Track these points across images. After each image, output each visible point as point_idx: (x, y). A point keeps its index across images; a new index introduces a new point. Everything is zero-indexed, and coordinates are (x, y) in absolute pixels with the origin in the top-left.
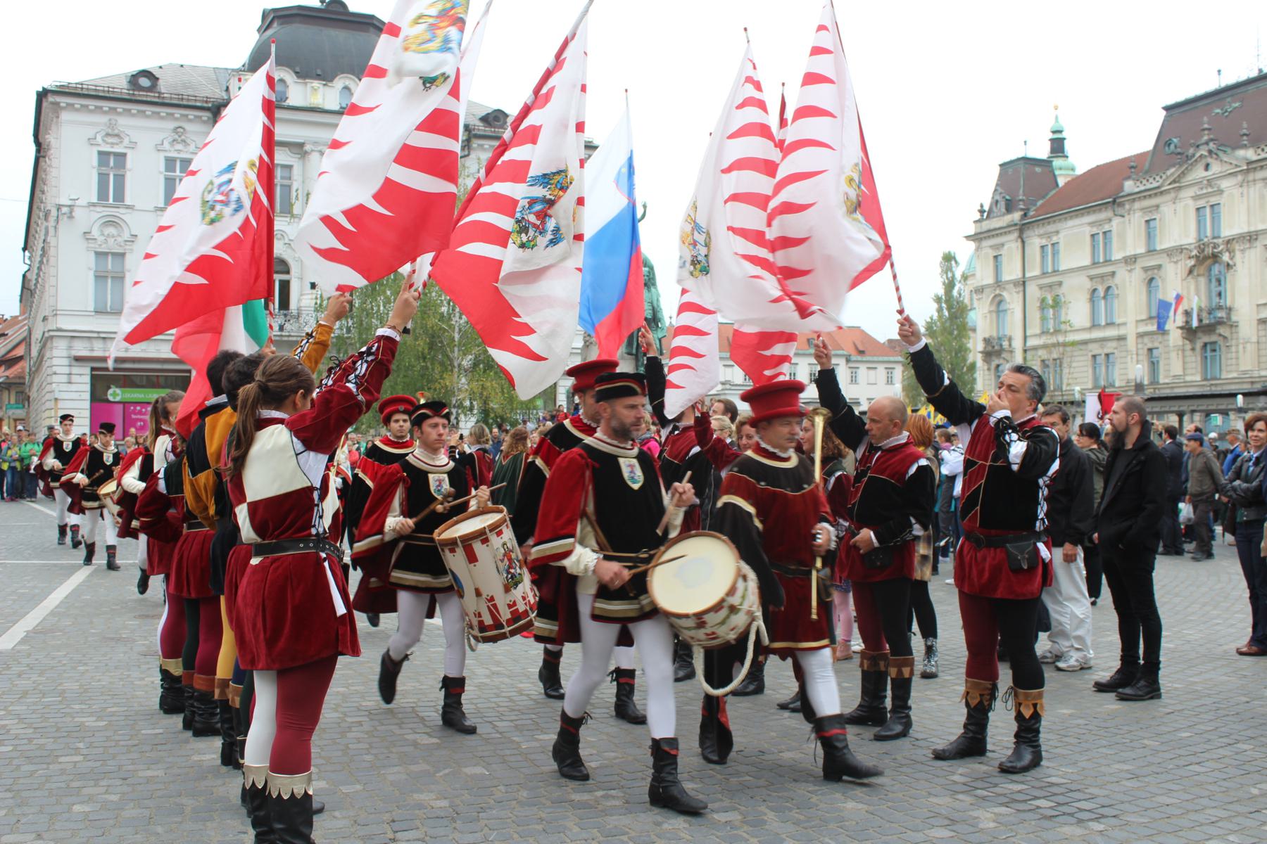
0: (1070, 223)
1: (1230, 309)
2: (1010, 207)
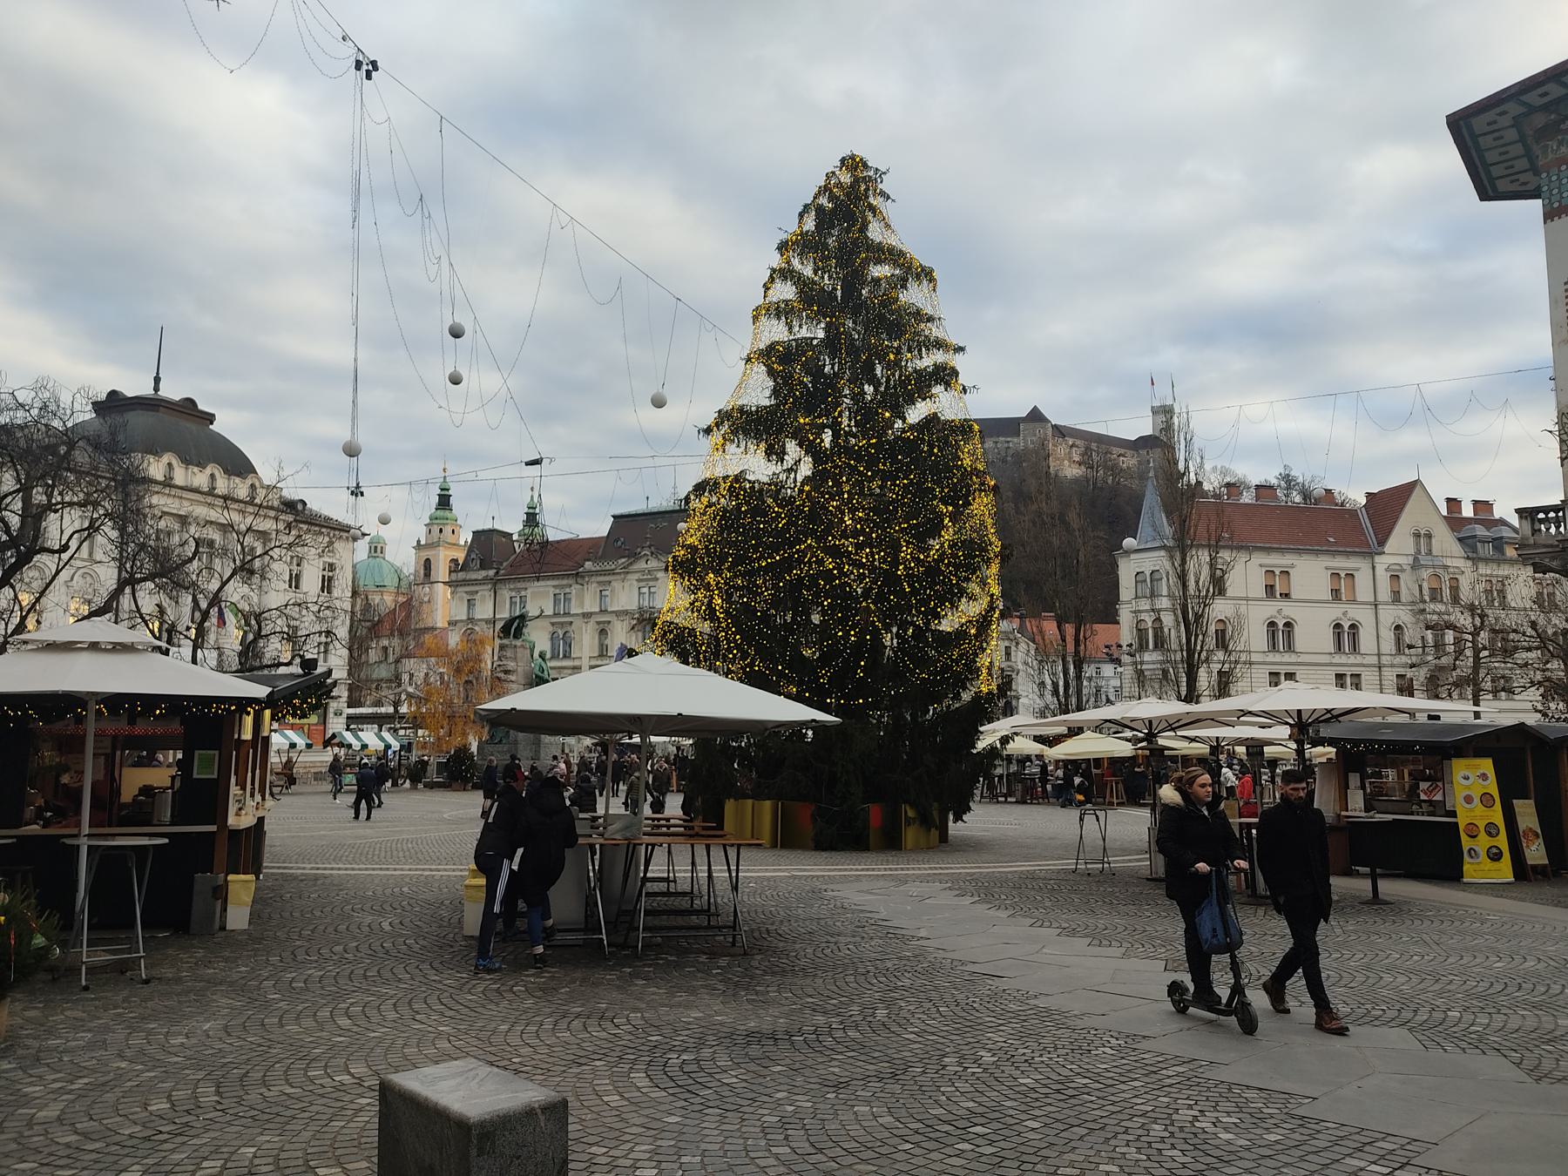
2: (482, 567)
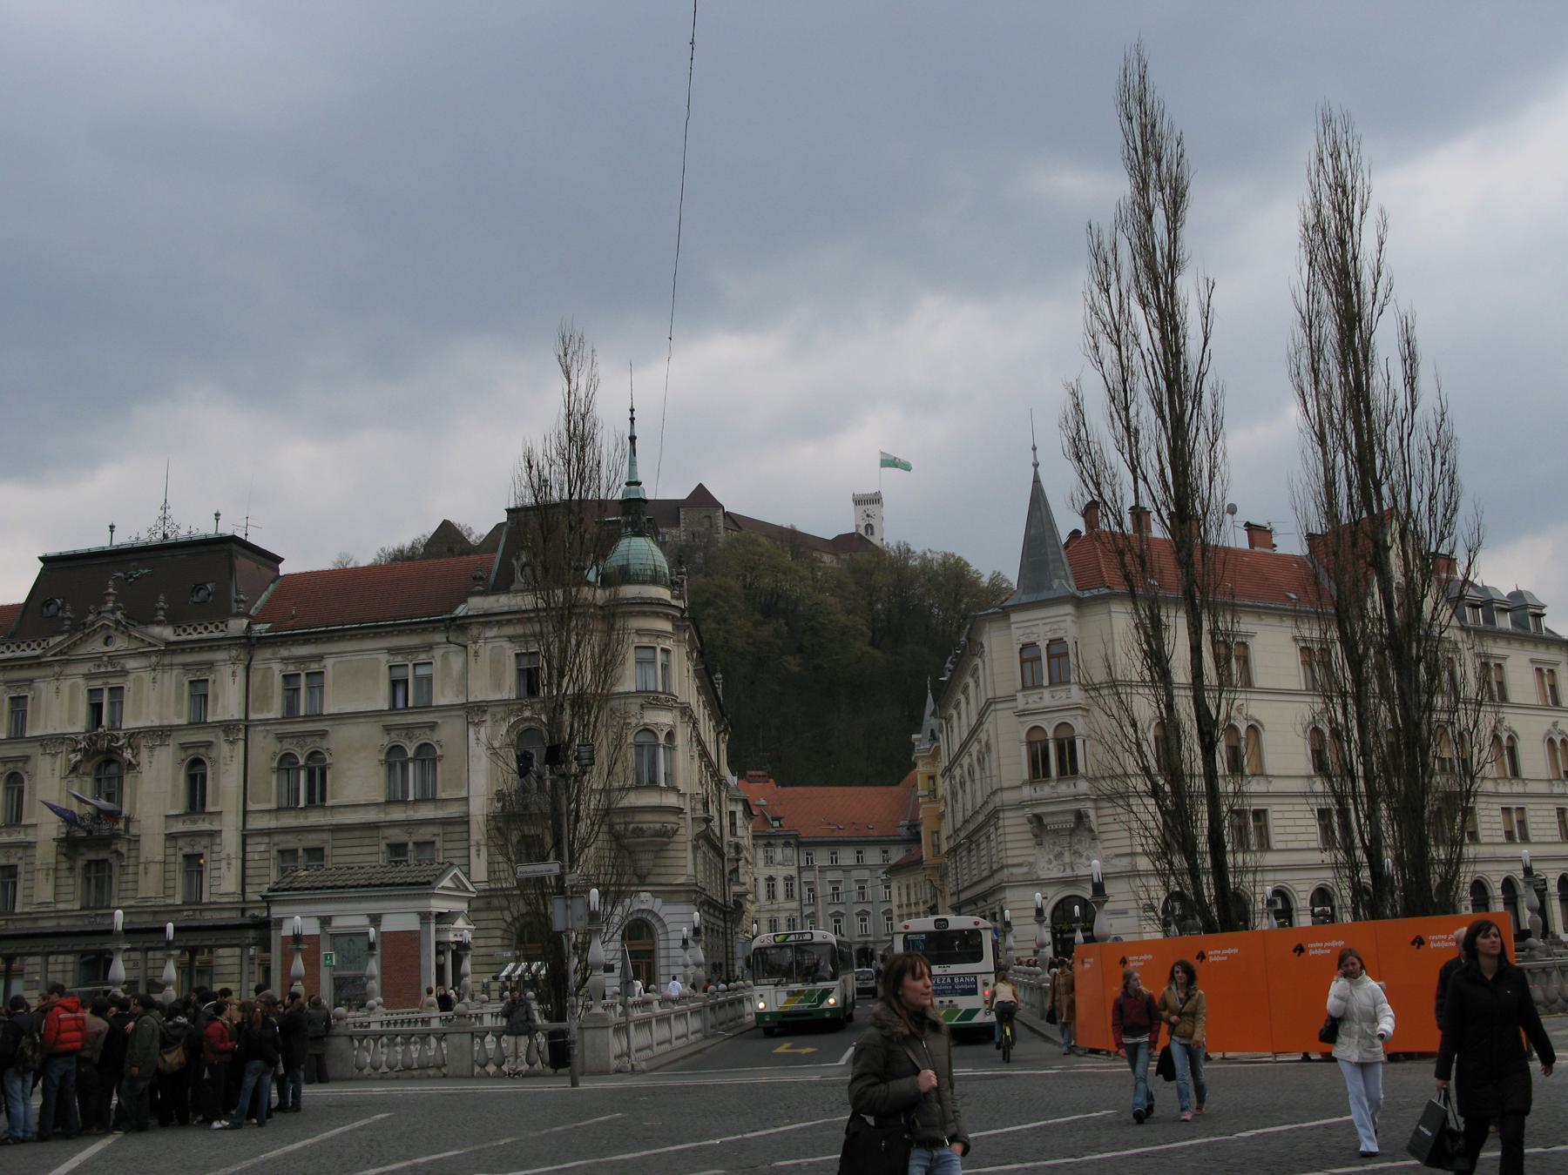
1: (128, 820)
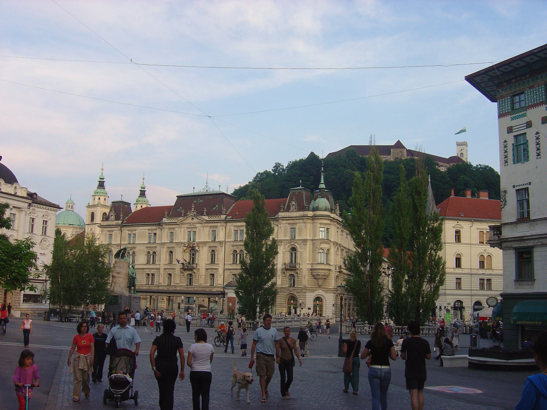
0: (141, 228)
2: (117, 218)
